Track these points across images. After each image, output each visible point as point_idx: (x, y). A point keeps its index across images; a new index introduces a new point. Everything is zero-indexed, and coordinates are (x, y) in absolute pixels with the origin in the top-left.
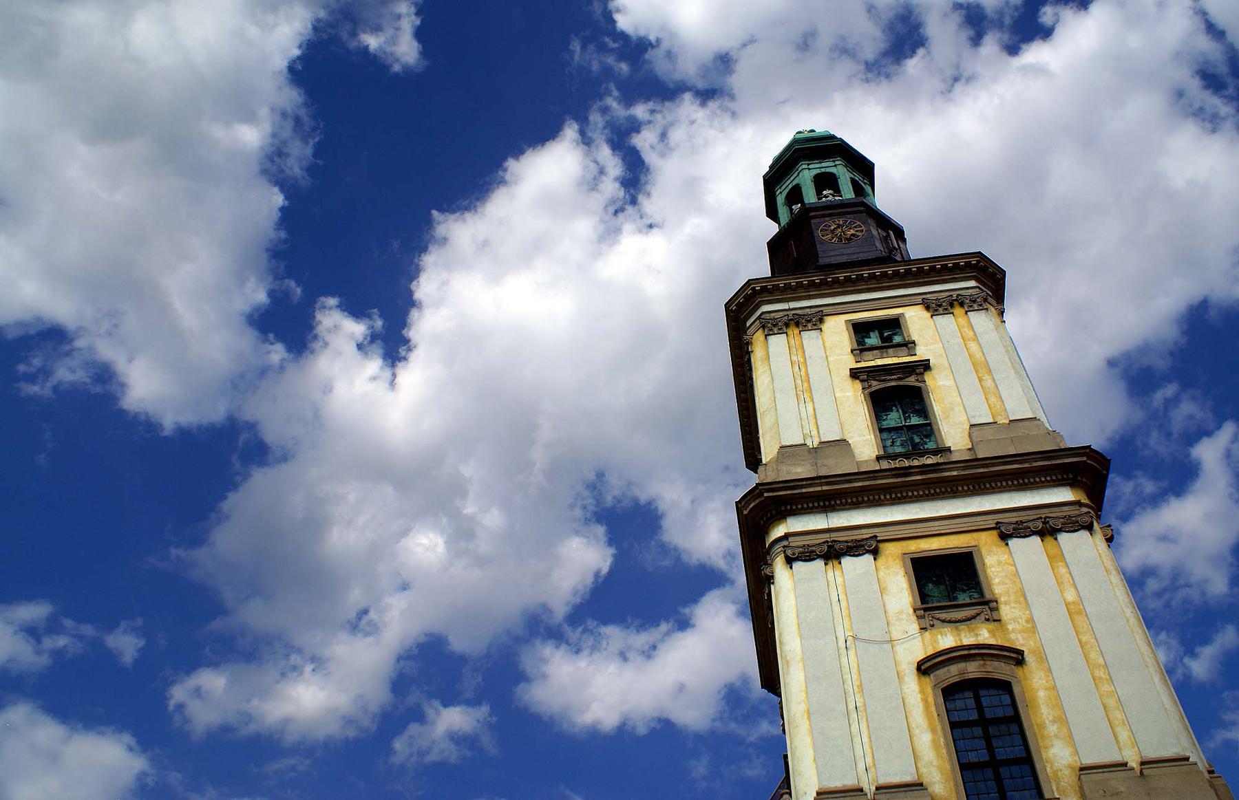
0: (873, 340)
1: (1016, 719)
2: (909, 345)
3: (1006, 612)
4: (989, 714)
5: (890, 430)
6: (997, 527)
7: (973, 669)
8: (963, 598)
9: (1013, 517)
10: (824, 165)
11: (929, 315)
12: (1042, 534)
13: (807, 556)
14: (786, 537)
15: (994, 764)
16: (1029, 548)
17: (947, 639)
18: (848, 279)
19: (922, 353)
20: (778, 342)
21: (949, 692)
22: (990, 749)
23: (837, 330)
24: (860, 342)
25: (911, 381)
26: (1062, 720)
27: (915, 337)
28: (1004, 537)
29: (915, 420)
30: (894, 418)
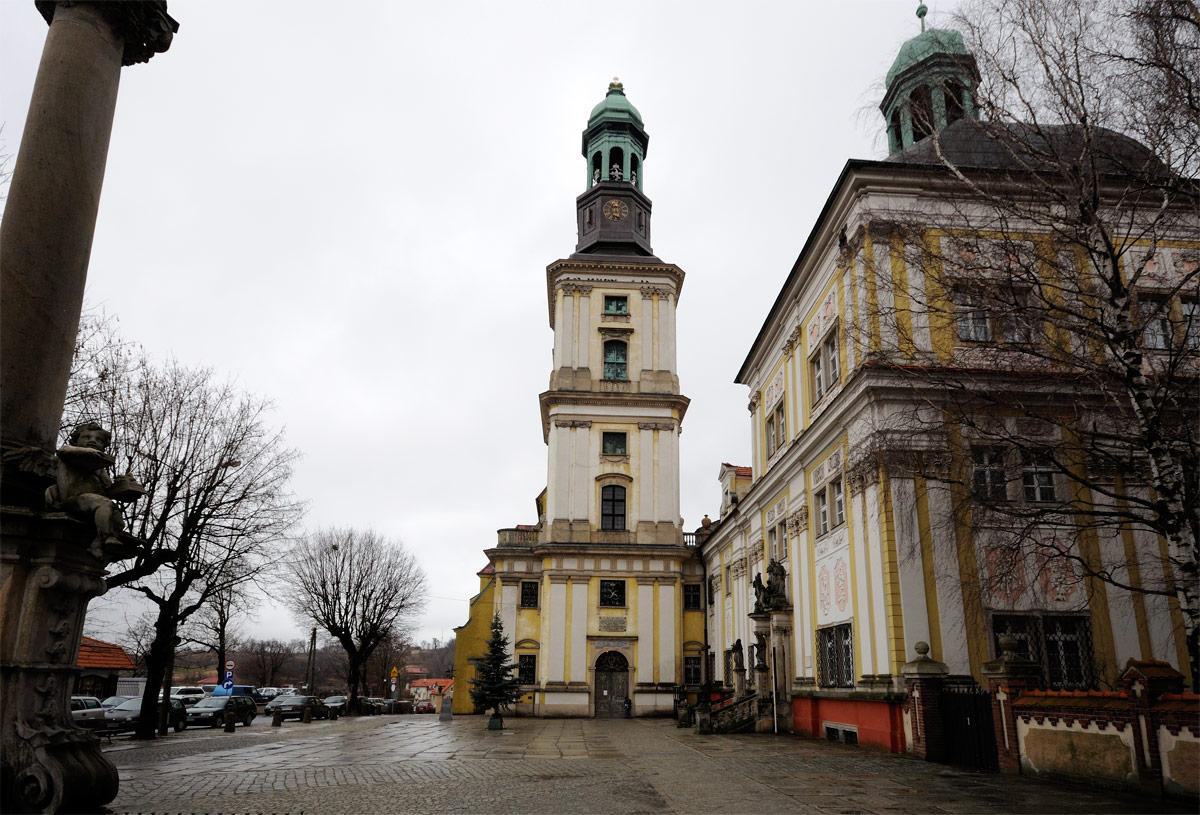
0: (613, 308)
1: (624, 501)
2: (627, 316)
3: (632, 461)
4: (616, 498)
5: (609, 363)
6: (638, 424)
7: (614, 482)
8: (619, 451)
9: (645, 421)
10: (619, 139)
11: (642, 297)
12: (654, 429)
13: (564, 425)
14: (557, 415)
15: (613, 515)
16: (648, 434)
17: (609, 469)
18: (608, 267)
19: (632, 324)
20: (569, 299)
21: (604, 489)
22: (614, 511)
23: (598, 296)
24: (607, 308)
25: (623, 339)
26: (639, 504)
27: (631, 312)
28: (640, 429)
29: (621, 360)
30: (612, 357)
